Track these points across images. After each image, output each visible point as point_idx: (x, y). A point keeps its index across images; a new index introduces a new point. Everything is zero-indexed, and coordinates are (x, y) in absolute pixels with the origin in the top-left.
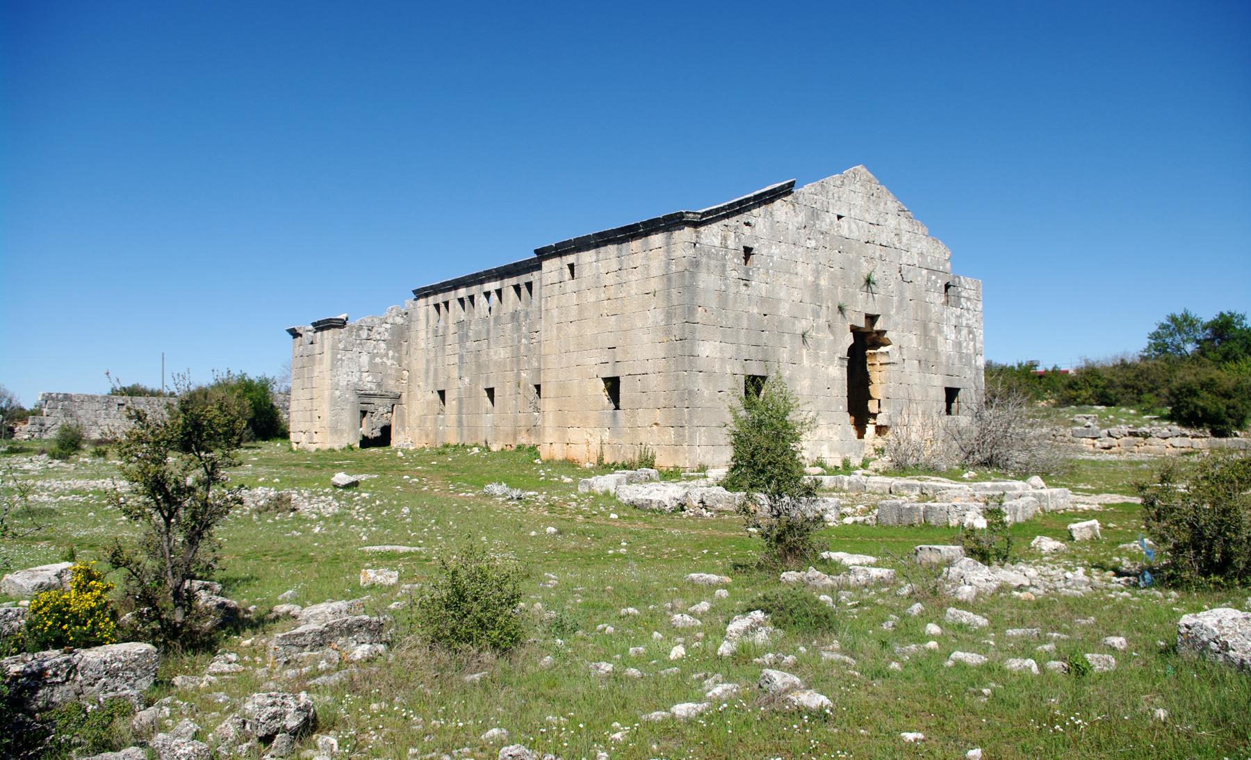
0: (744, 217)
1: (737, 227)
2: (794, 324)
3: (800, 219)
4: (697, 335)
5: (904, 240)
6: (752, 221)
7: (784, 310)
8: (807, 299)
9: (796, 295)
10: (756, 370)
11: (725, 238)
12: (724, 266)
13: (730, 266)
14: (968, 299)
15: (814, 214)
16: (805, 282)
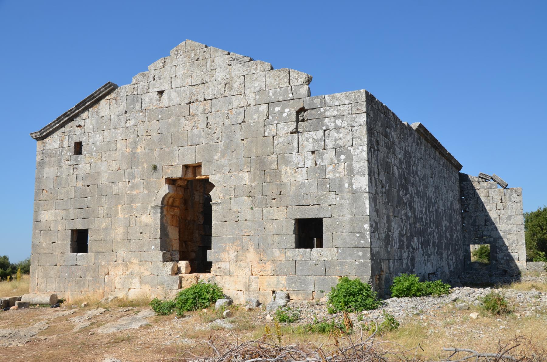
0: (77, 122)
1: (71, 131)
2: (111, 188)
3: (121, 108)
4: (41, 209)
5: (236, 85)
6: (82, 123)
7: (104, 180)
8: (124, 167)
9: (114, 166)
10: (80, 226)
11: (62, 141)
12: (61, 159)
13: (65, 158)
14: (341, 117)
15: (135, 98)
16: (123, 155)
